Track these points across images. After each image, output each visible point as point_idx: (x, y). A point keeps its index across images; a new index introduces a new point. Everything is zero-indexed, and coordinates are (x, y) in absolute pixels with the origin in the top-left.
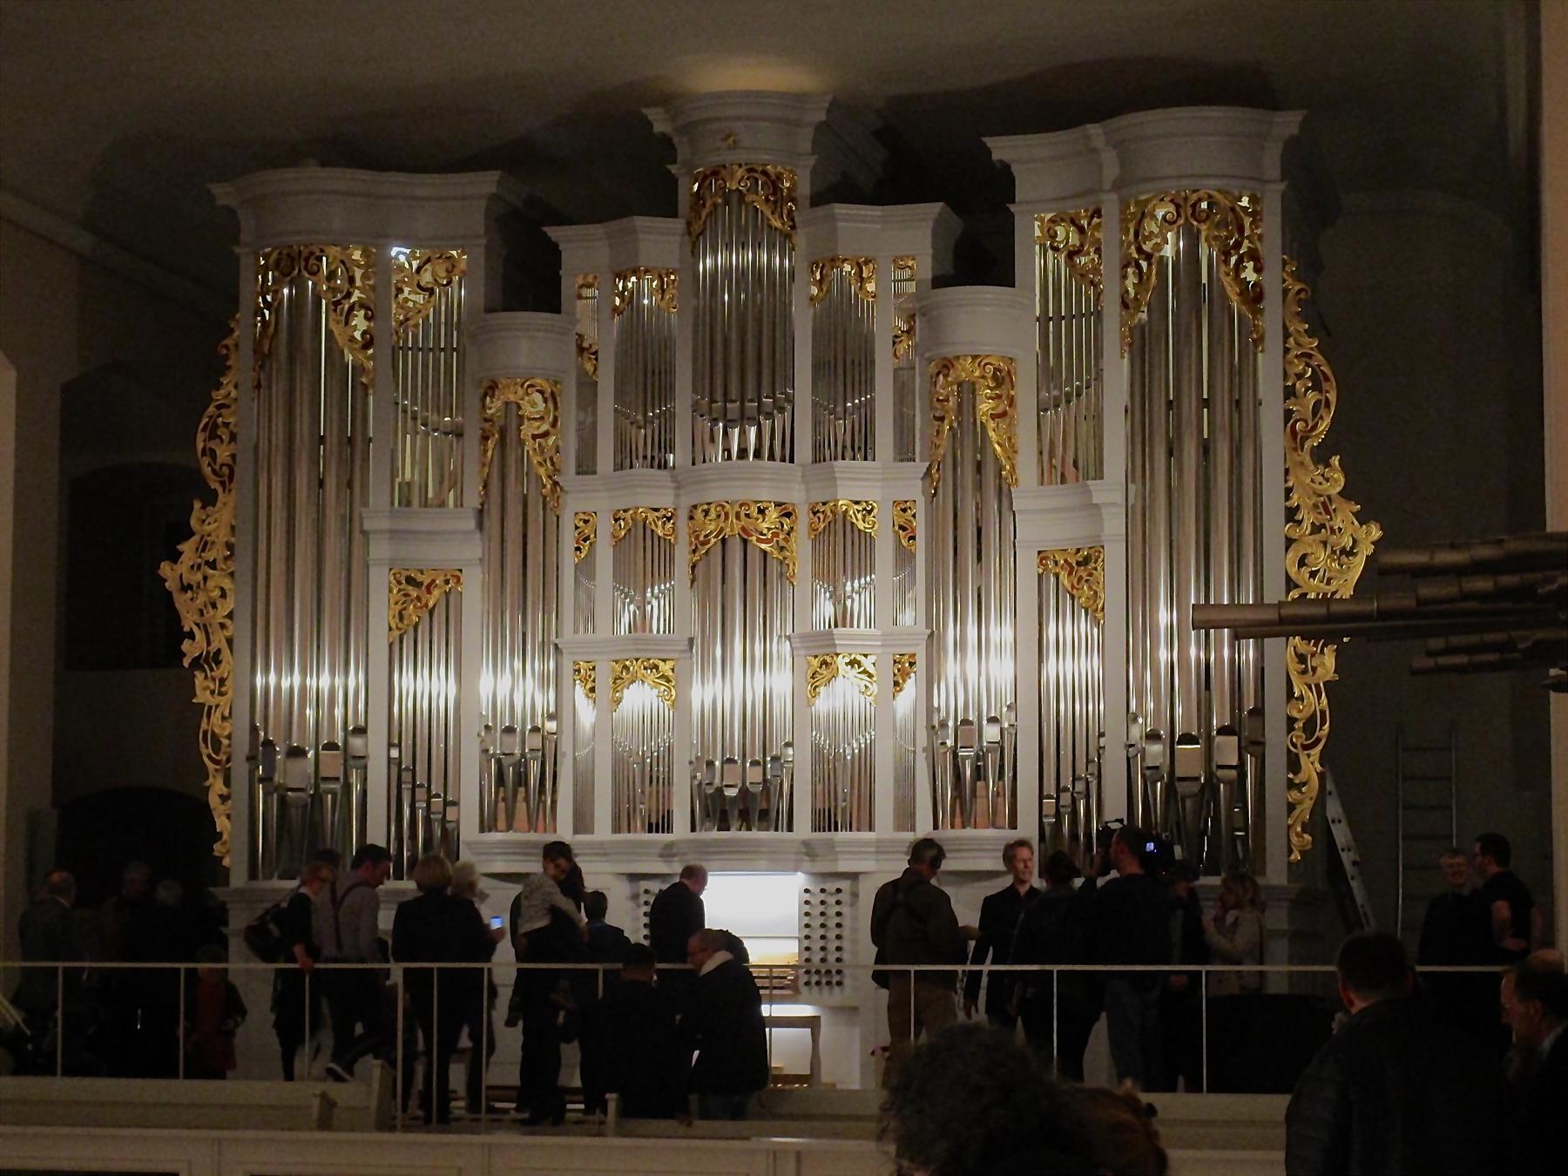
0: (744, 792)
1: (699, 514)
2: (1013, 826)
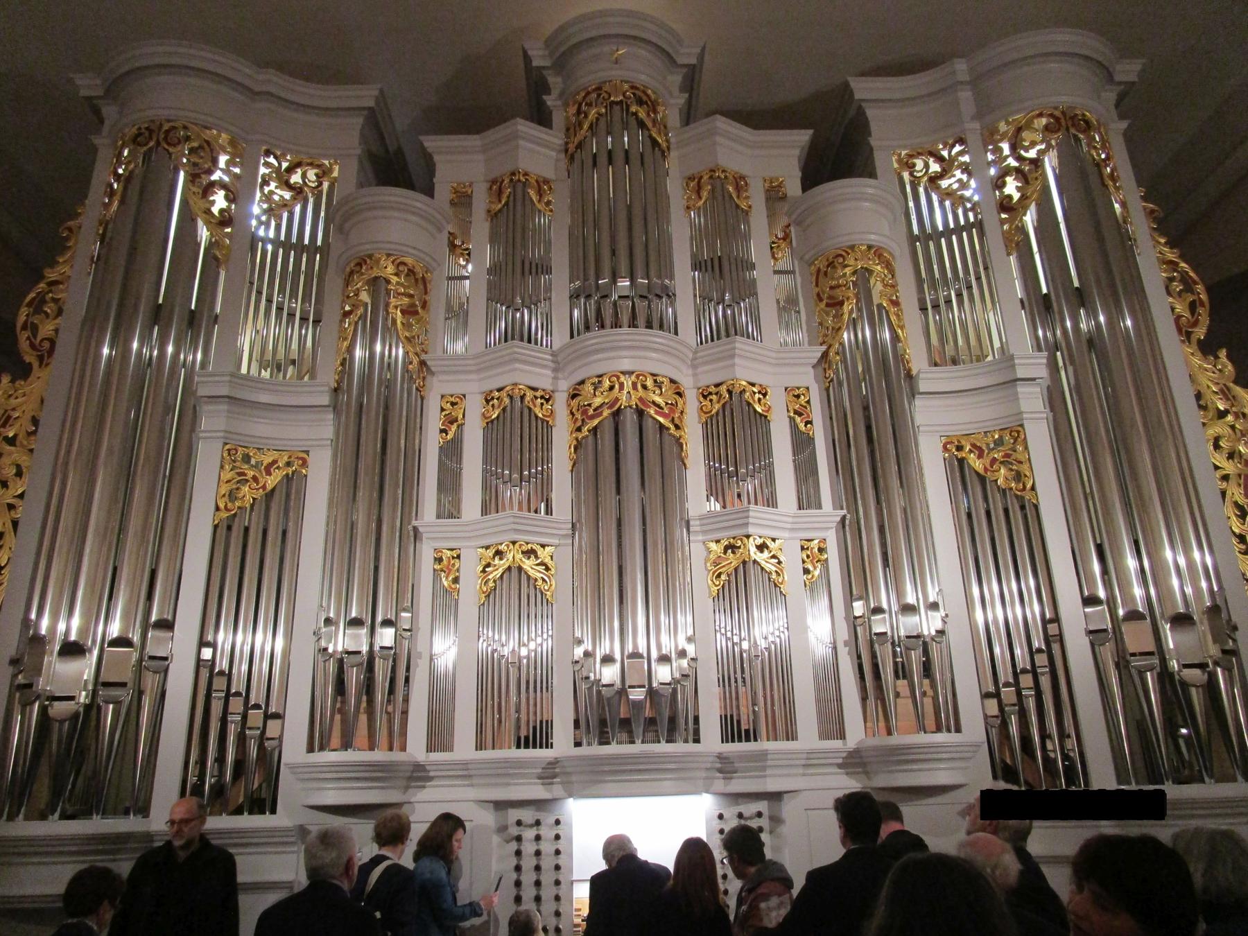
0: (652, 693)
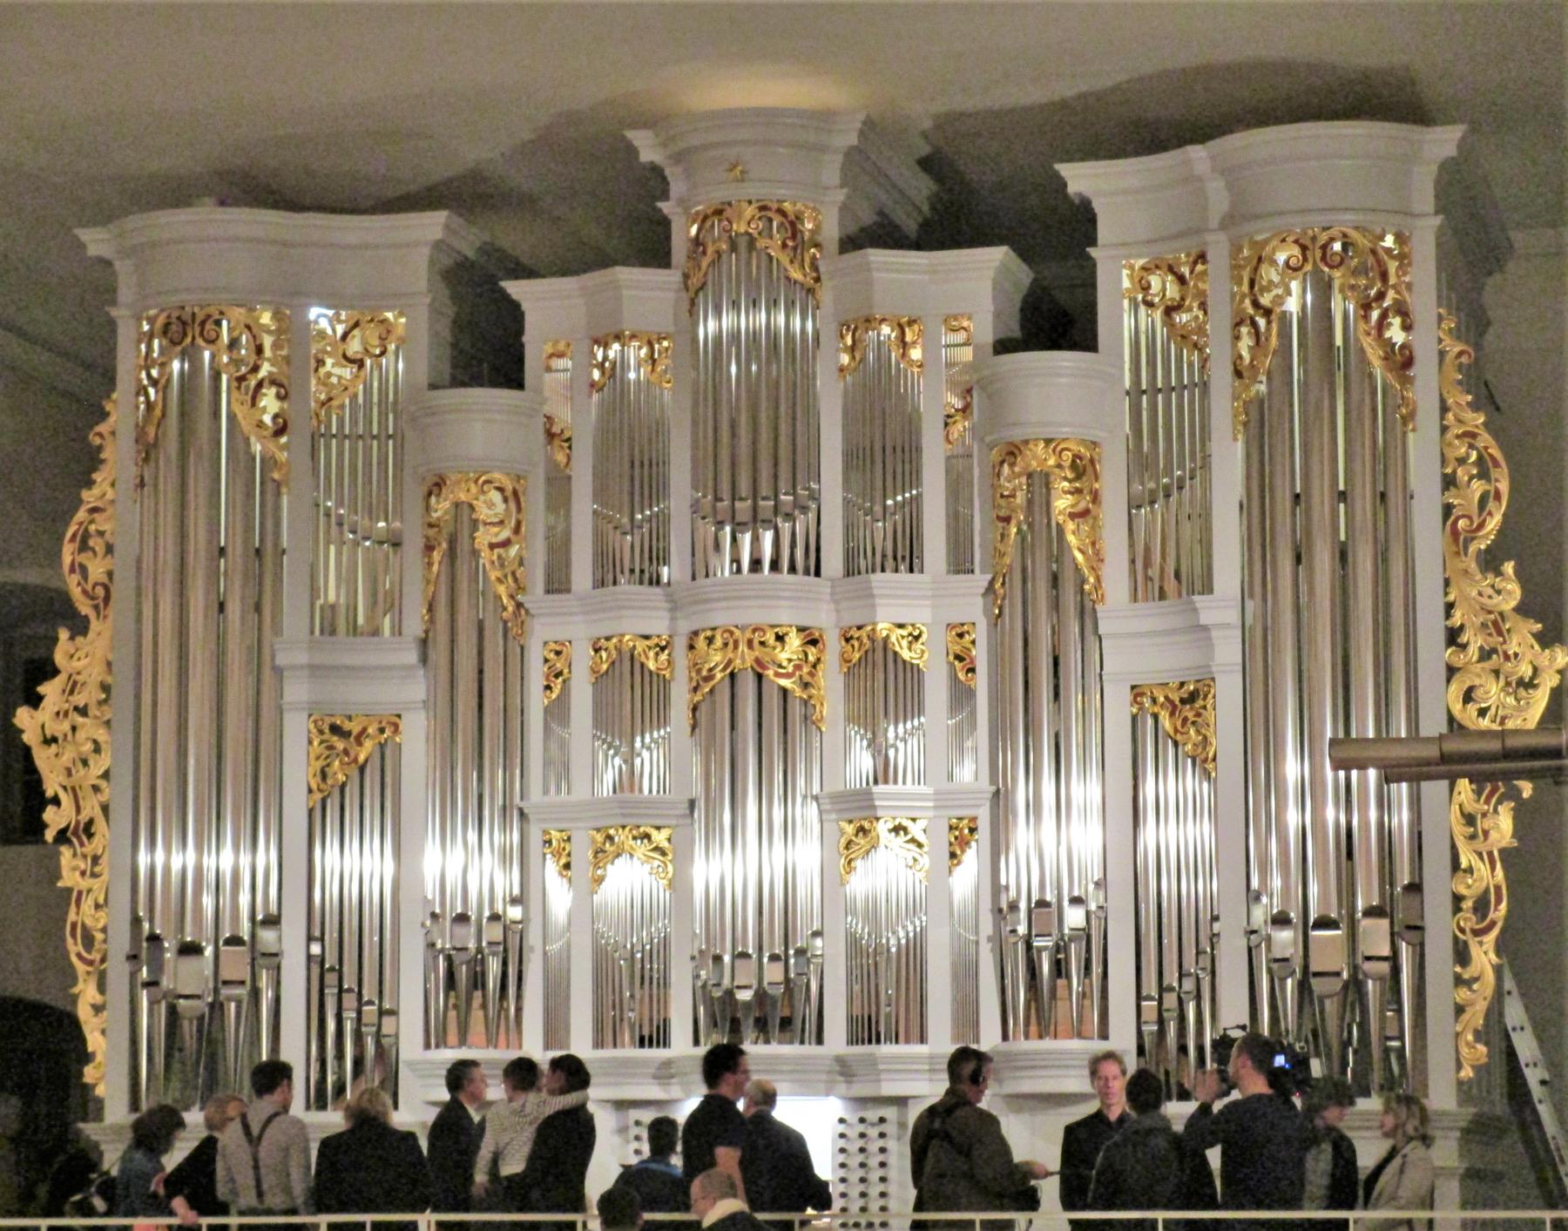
0: (761, 996)
1: (701, 643)
2: (1104, 1035)
